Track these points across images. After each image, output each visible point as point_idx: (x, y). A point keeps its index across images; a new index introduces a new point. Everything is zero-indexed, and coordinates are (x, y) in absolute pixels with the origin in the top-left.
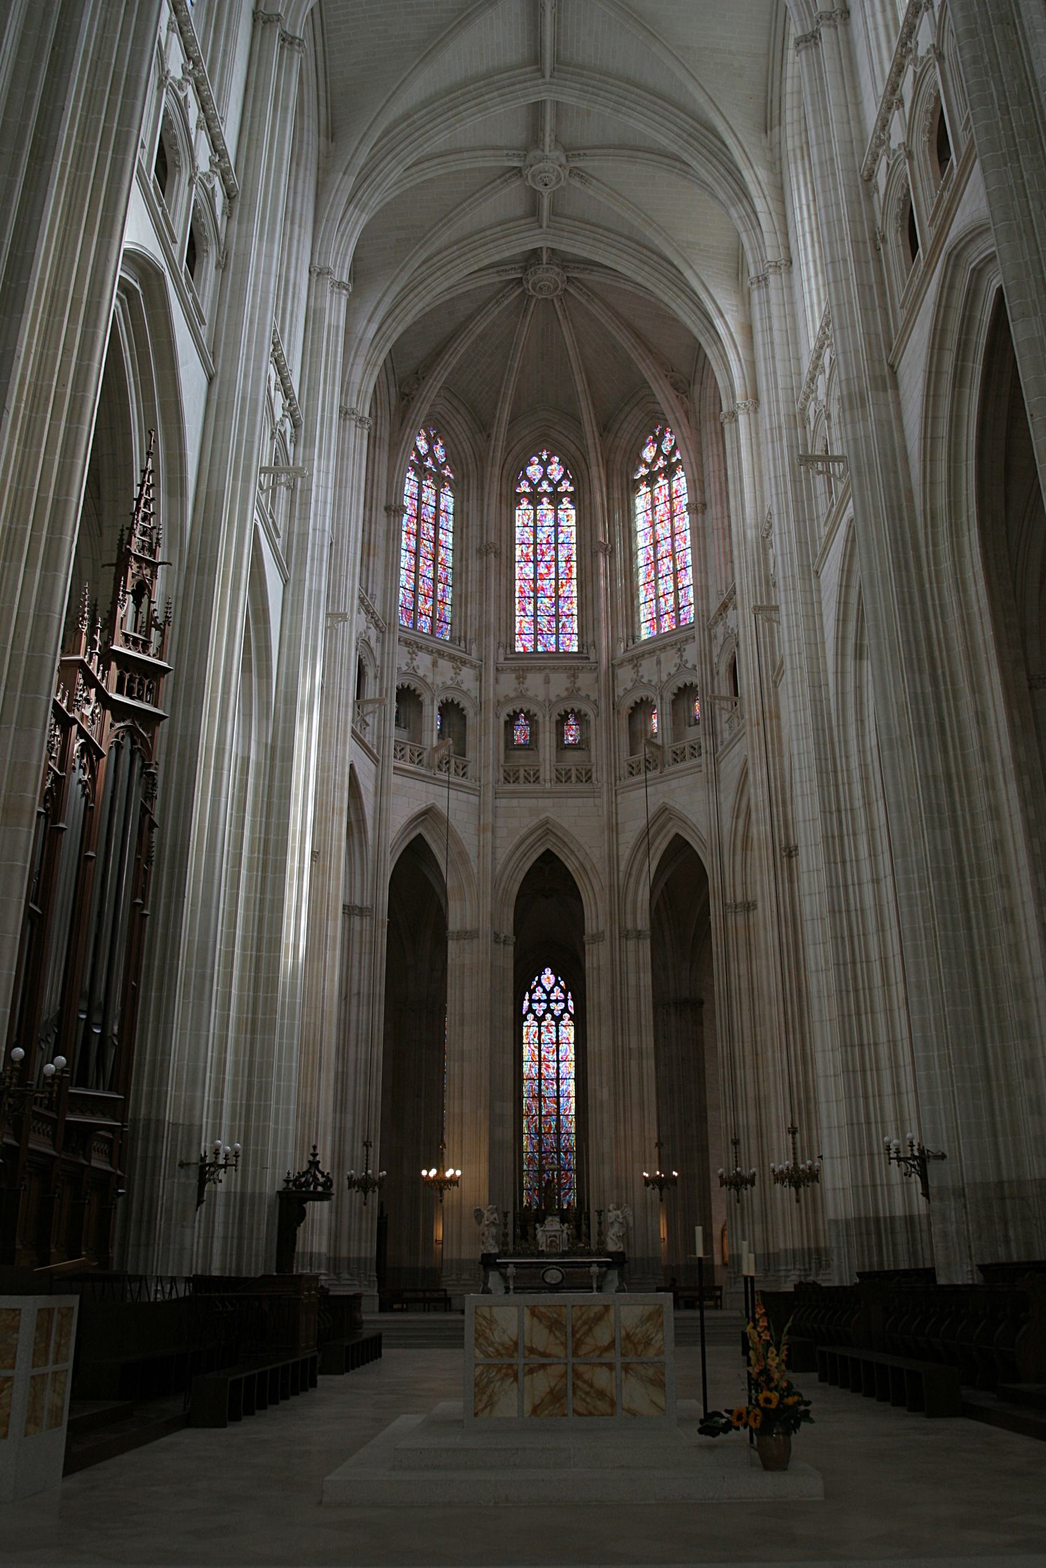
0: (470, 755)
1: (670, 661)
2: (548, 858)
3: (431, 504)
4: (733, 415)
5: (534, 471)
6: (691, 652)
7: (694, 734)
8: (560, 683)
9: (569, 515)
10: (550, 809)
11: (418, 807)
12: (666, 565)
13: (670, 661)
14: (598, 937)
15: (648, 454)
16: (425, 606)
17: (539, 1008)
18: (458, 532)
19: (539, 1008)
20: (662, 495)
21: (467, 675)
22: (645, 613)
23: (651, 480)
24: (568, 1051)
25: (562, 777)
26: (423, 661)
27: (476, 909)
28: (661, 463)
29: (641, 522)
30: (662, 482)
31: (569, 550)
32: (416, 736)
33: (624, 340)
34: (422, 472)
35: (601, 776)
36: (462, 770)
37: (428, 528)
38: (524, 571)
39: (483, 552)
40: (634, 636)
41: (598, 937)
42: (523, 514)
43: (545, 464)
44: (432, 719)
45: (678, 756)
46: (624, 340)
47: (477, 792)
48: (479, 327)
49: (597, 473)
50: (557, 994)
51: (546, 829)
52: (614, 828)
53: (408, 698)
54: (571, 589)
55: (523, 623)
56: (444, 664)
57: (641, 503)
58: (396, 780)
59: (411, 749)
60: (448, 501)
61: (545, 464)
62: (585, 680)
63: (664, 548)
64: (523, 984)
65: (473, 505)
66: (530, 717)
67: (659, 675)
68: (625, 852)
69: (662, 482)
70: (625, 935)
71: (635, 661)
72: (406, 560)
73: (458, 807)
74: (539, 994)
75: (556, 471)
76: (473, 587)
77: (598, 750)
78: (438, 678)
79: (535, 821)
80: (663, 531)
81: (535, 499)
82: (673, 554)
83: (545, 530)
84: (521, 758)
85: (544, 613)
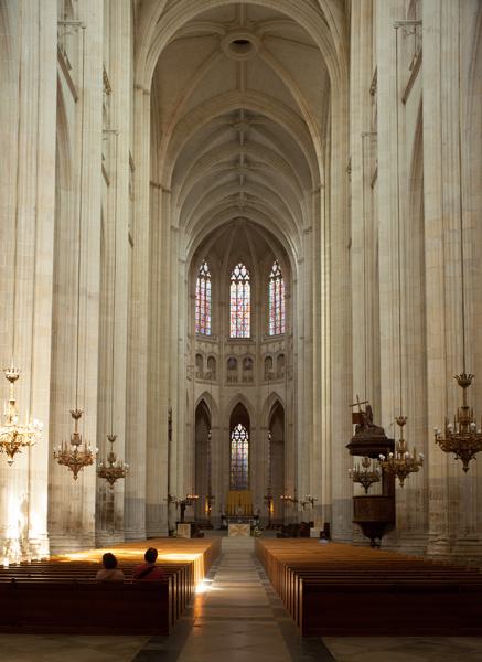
0: (217, 373)
1: (277, 346)
2: (240, 404)
3: (204, 286)
4: (296, 282)
5: (237, 271)
6: (283, 344)
7: (283, 369)
8: (244, 349)
9: (248, 287)
10: (241, 390)
11: (201, 393)
12: (278, 311)
13: (277, 346)
14: (254, 429)
15: (274, 268)
16: (202, 325)
17: (237, 437)
18: (212, 296)
19: (237, 437)
20: (278, 285)
21: (216, 347)
22: (271, 326)
23: (275, 279)
24: (246, 451)
25: (244, 379)
26: (203, 344)
27: (219, 419)
28: (278, 273)
29: (271, 293)
30: (278, 280)
31: (248, 301)
32: (201, 369)
33: (267, 239)
34: (201, 277)
35: (256, 381)
36: (215, 379)
37: (203, 297)
38: (233, 308)
39: (221, 304)
40: (268, 335)
41: (254, 429)
42: (233, 287)
43: (240, 269)
44: (205, 361)
45: (278, 377)
46: (267, 239)
47: (220, 385)
48: (219, 234)
49: (256, 277)
50: (243, 432)
51: (240, 396)
52: (259, 397)
53: (198, 355)
54: (248, 315)
55: (233, 327)
56: (210, 345)
57: (271, 286)
58: (198, 385)
59: (200, 375)
60: (209, 286)
61: (240, 269)
62: (252, 348)
63: (278, 305)
64: (232, 428)
65: (217, 287)
66: (235, 360)
67: (273, 348)
68: (262, 403)
69: (278, 280)
70: (261, 428)
71: (267, 344)
72: (197, 310)
73: (214, 391)
74: (237, 432)
75: (244, 271)
76: (217, 317)
77: (255, 368)
78: (207, 349)
79: (234, 394)
80: (278, 298)
81: (237, 282)
82: (280, 307)
83: (240, 293)
84: (232, 373)
85: (240, 324)
